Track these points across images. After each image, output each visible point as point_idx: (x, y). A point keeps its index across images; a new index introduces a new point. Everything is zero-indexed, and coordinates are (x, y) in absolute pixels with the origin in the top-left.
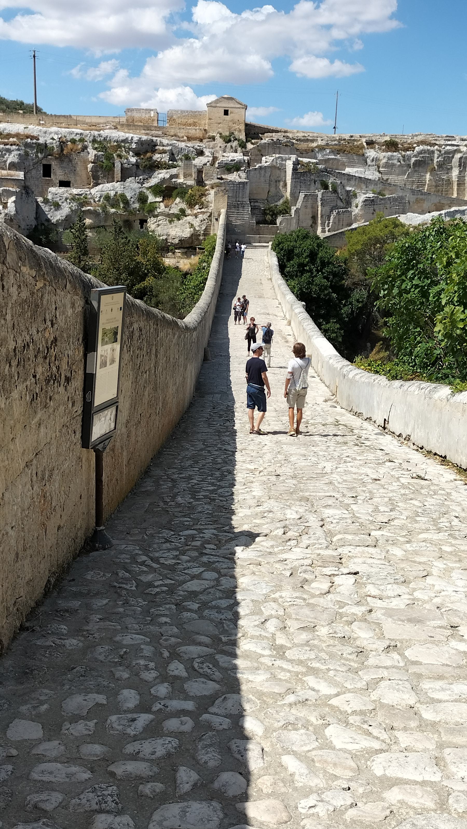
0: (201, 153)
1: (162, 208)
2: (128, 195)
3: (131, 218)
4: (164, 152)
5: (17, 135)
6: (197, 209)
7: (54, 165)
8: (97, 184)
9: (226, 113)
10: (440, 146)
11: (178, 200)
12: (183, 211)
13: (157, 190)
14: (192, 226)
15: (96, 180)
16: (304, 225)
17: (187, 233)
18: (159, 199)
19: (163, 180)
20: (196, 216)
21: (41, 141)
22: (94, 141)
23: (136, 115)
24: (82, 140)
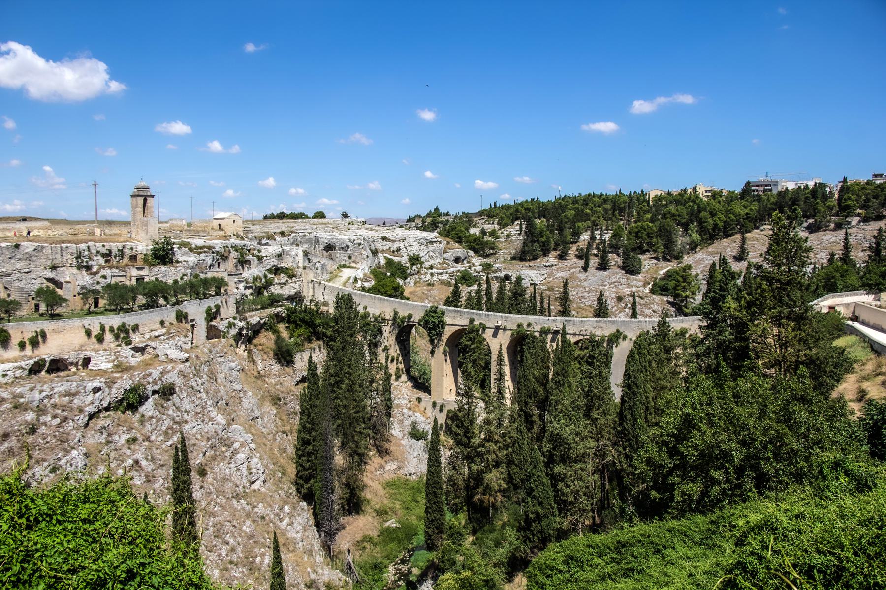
1: (276, 281)
17: (293, 292)
23: (175, 222)
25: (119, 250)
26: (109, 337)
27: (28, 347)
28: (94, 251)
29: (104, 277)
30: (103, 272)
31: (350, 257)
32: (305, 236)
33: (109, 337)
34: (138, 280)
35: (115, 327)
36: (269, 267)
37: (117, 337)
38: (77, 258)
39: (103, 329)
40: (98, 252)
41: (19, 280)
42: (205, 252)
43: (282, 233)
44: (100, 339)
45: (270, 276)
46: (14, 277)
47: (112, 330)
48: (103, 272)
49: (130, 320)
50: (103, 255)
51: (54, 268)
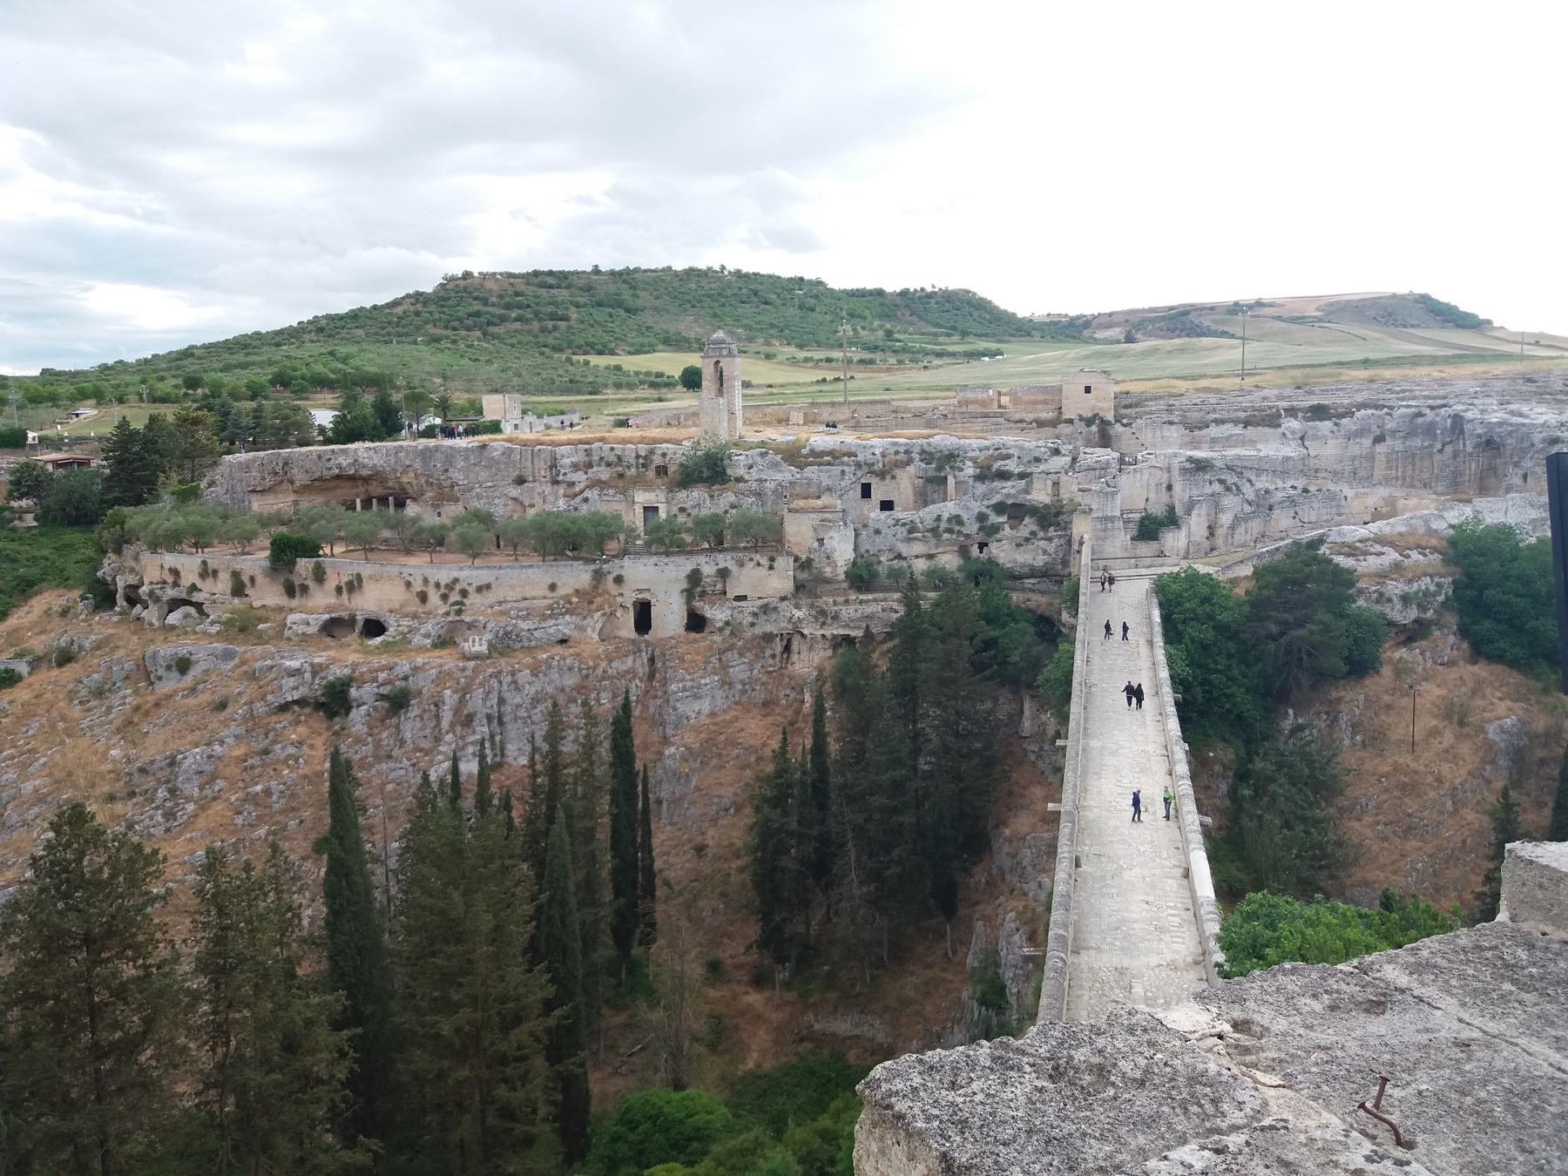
0: (1057, 452)
2: (965, 517)
3: (969, 542)
4: (1008, 457)
5: (831, 453)
6: (1052, 532)
7: (874, 481)
8: (926, 504)
9: (1088, 390)
10: (1391, 408)
11: (1027, 520)
12: (1033, 533)
13: (1000, 508)
14: (1045, 552)
15: (923, 499)
16: (1197, 539)
18: (1002, 519)
19: (1008, 496)
20: (1050, 540)
21: (860, 458)
22: (923, 452)
23: (970, 395)
24: (906, 452)
25: (638, 457)
26: (434, 597)
27: (345, 595)
28: (596, 458)
29: (586, 500)
30: (587, 494)
31: (1525, 477)
32: (1420, 414)
33: (434, 597)
34: (645, 509)
35: (443, 583)
36: (994, 501)
37: (445, 597)
38: (551, 468)
39: (426, 581)
40: (602, 459)
41: (479, 497)
42: (829, 464)
43: (1319, 412)
44: (423, 597)
45: (994, 519)
46: (473, 493)
47: (438, 585)
48: (587, 494)
49: (471, 574)
50: (608, 465)
51: (521, 481)
